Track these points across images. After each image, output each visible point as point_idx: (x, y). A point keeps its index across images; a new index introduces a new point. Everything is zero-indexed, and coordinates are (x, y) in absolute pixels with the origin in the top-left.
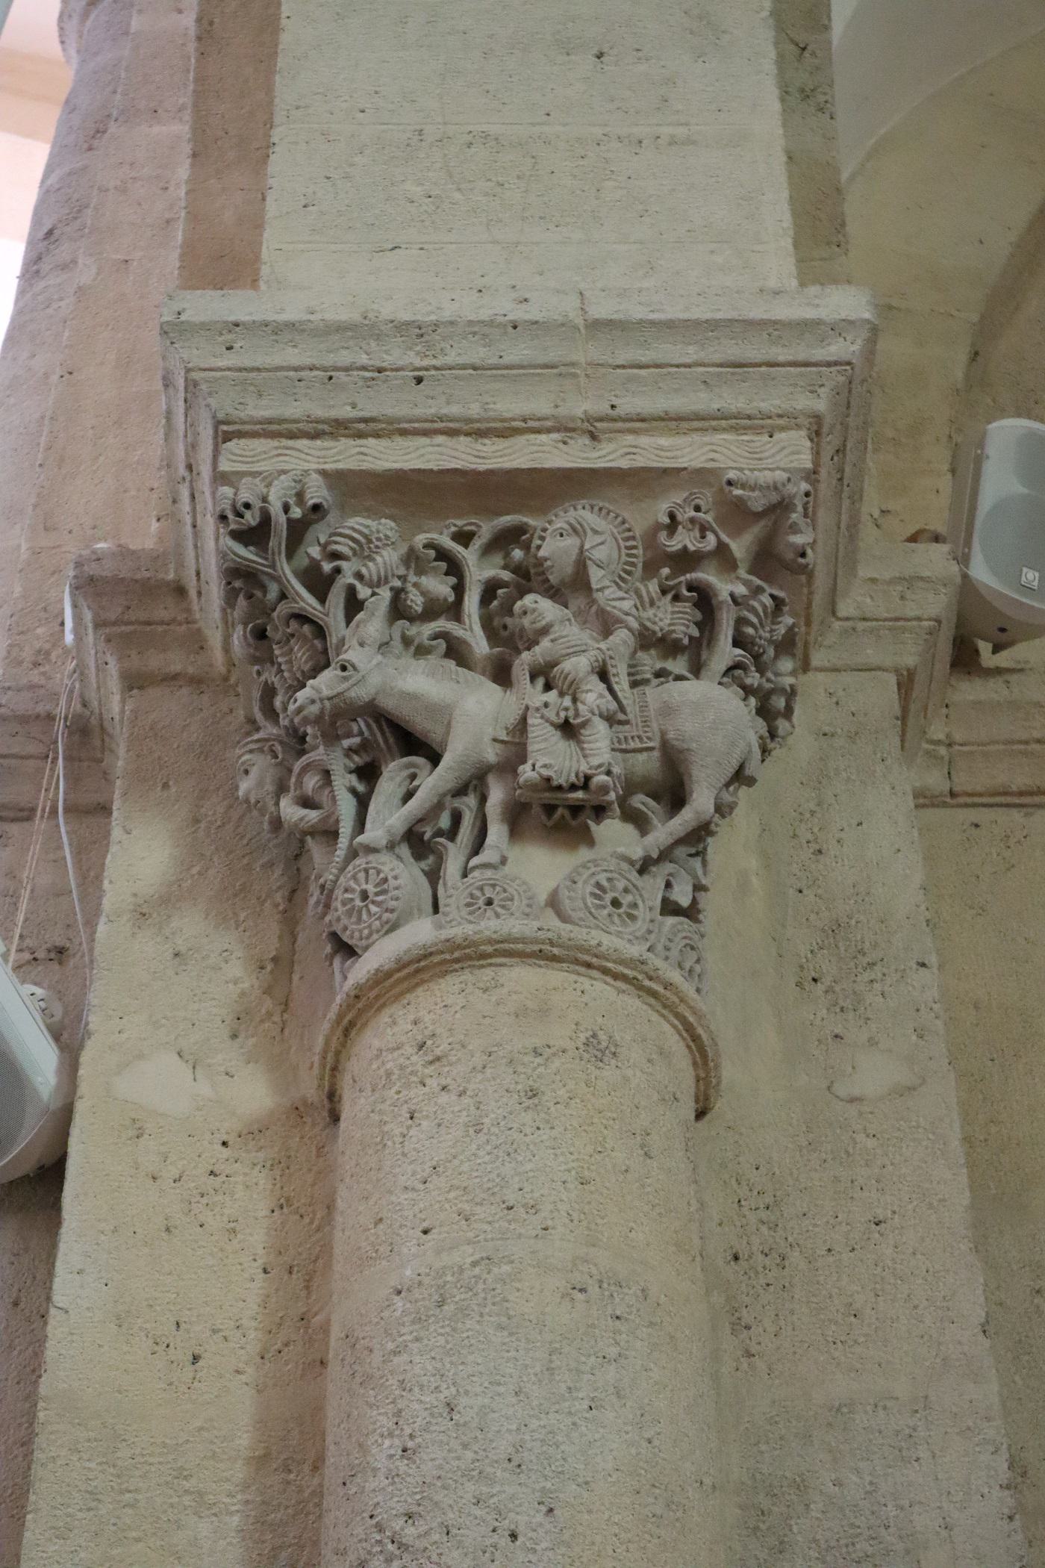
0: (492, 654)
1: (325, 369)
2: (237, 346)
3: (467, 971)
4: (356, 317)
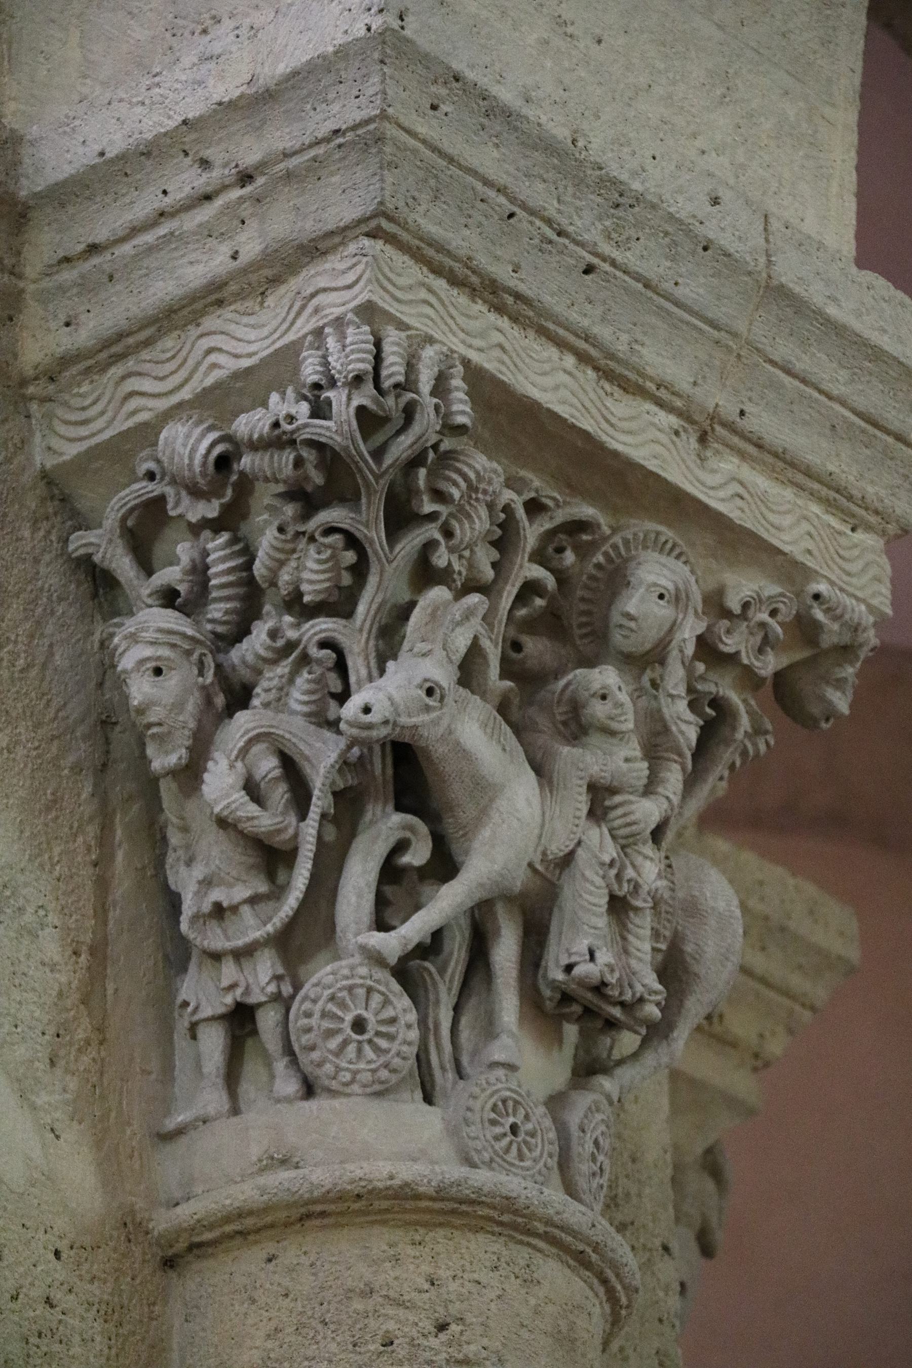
1: (513, 200)
2: (444, 108)
3: (502, 1239)
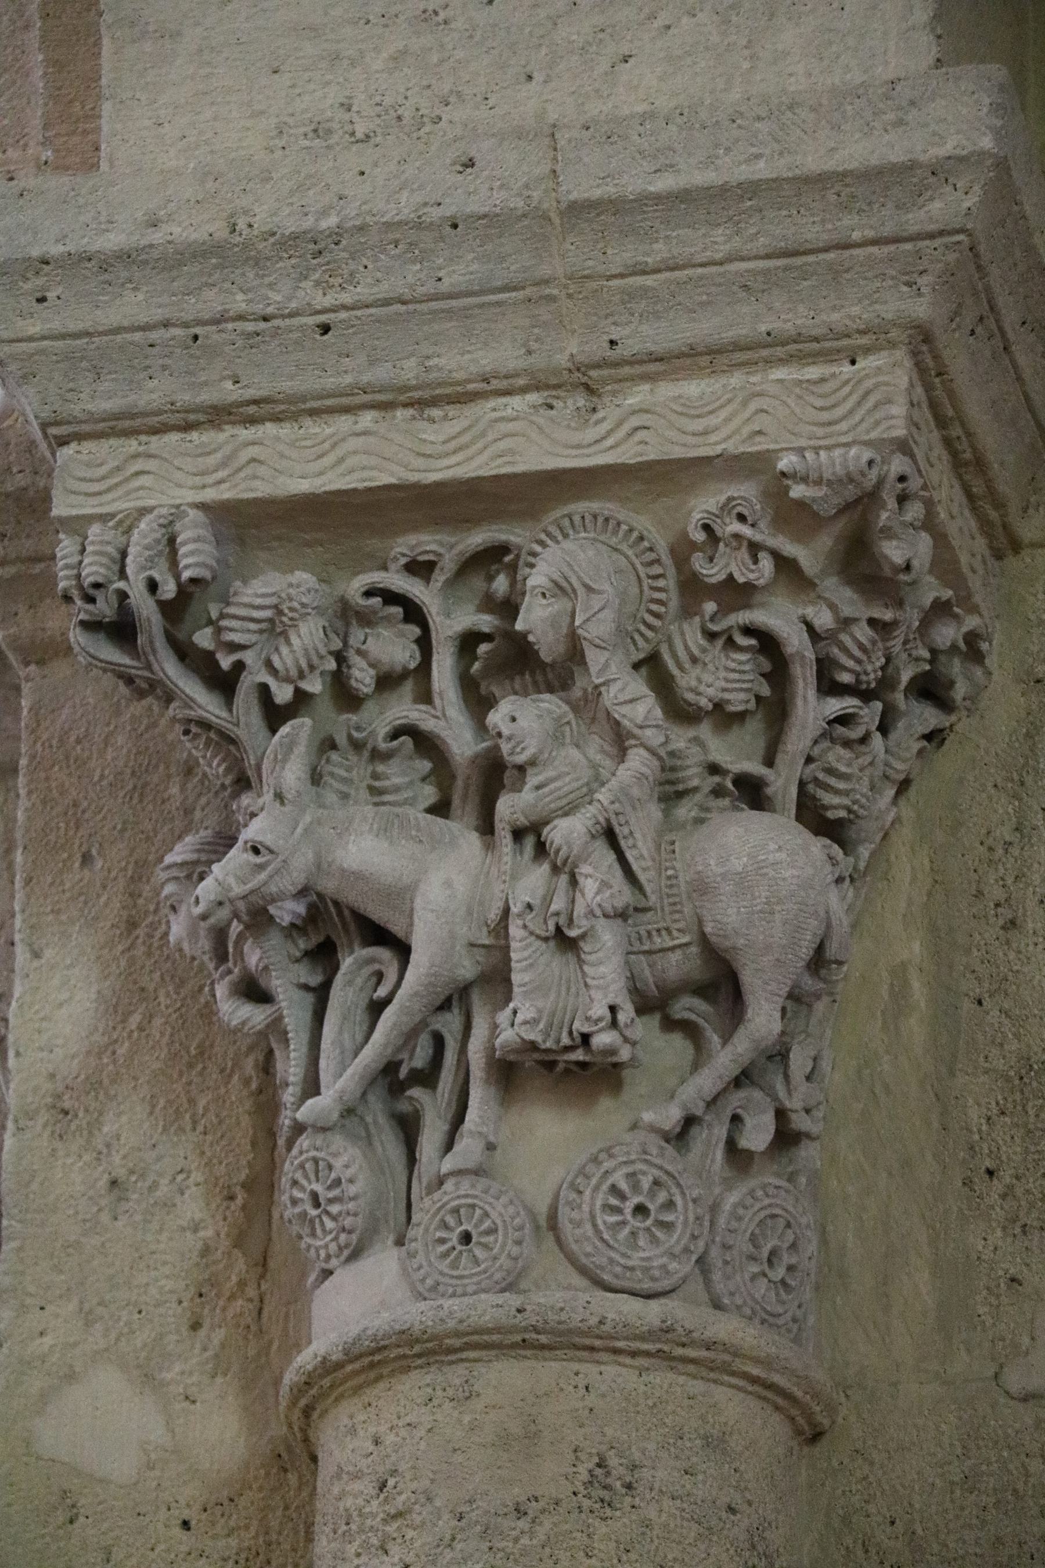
1: (186, 325)
2: (51, 295)
4: (219, 229)
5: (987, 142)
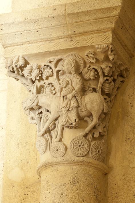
0: (60, 86)
5: (120, 4)
